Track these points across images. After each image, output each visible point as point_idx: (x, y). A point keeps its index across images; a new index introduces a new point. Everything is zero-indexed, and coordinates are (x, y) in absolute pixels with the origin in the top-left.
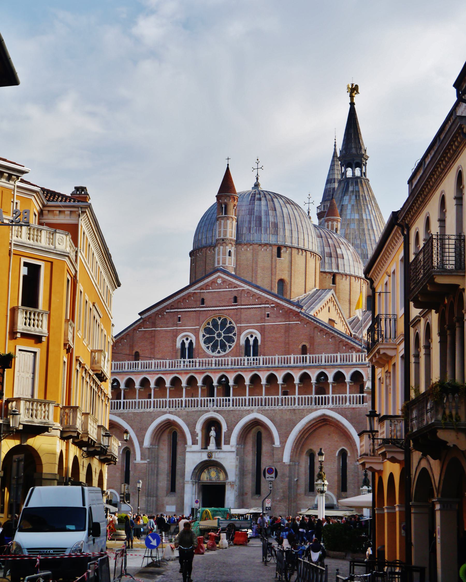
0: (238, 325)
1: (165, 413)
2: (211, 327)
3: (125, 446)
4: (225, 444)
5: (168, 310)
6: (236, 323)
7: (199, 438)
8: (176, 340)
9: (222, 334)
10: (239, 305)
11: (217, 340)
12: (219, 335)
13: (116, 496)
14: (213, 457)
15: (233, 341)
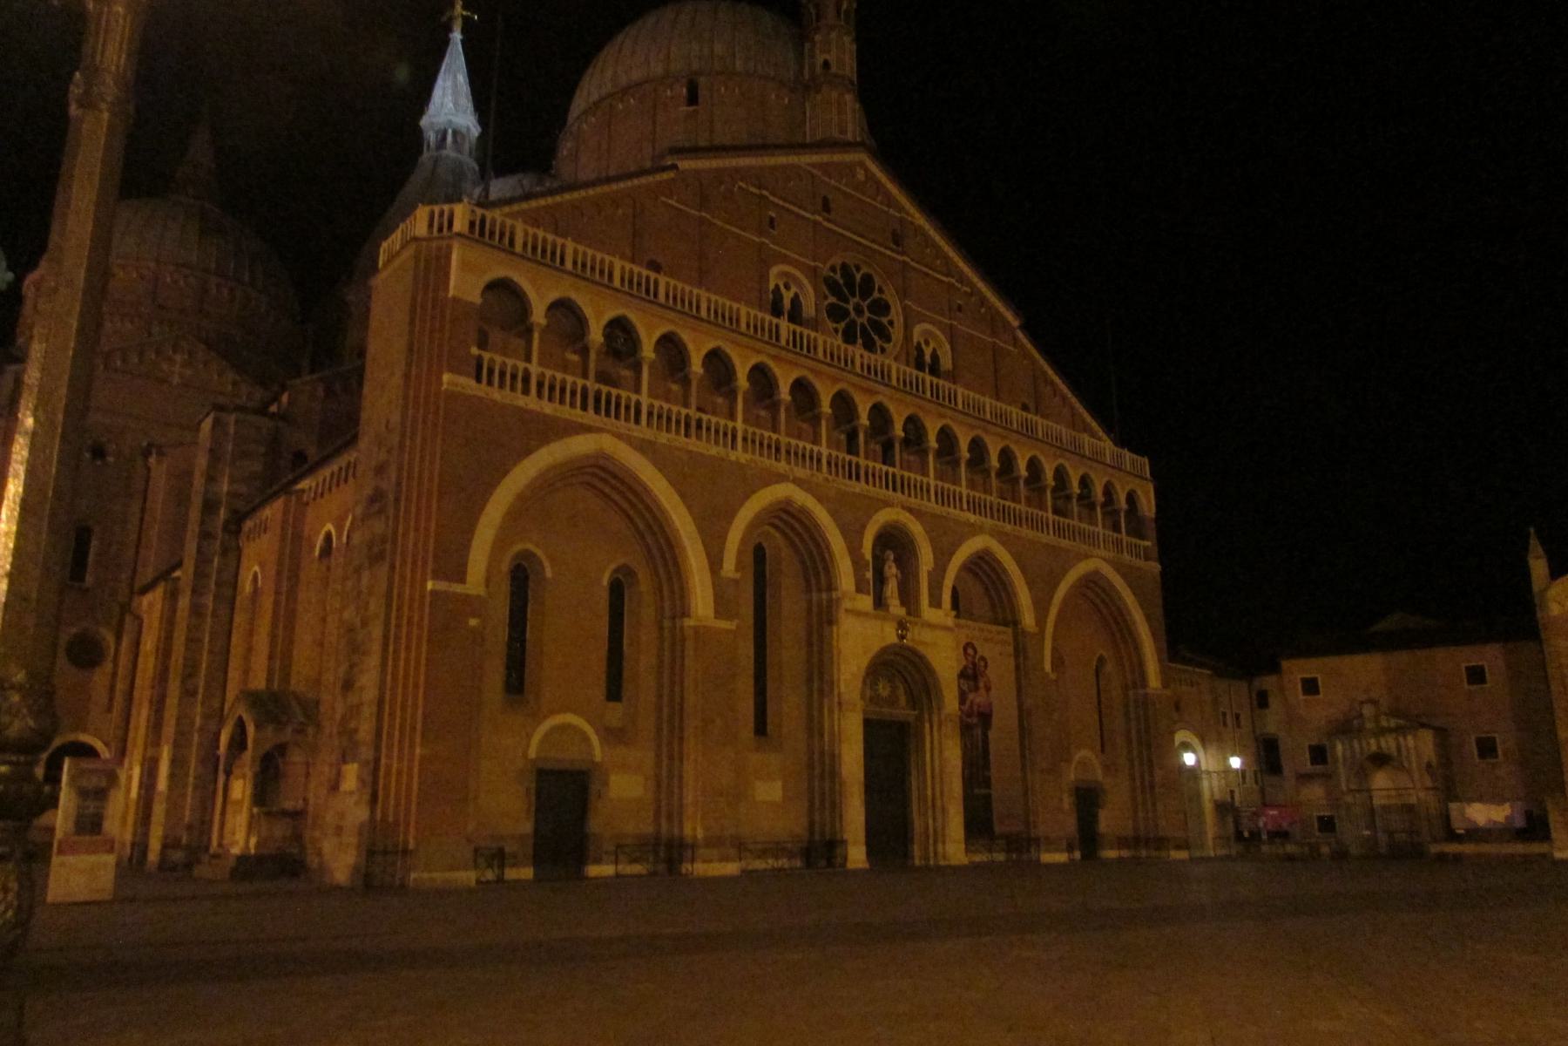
0: (906, 302)
1: (781, 478)
2: (838, 277)
3: (621, 561)
4: (931, 605)
5: (742, 181)
6: (904, 293)
7: (869, 575)
8: (768, 274)
9: (866, 309)
10: (908, 256)
11: (853, 322)
12: (859, 311)
13: (585, 739)
14: (909, 635)
15: (888, 339)
